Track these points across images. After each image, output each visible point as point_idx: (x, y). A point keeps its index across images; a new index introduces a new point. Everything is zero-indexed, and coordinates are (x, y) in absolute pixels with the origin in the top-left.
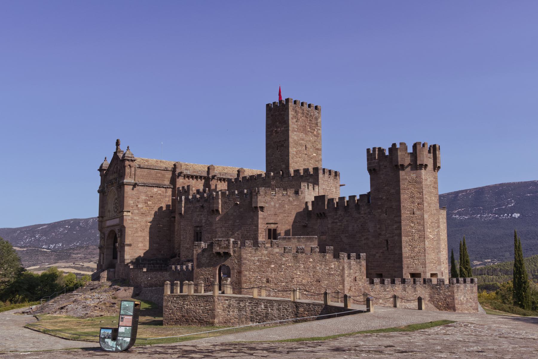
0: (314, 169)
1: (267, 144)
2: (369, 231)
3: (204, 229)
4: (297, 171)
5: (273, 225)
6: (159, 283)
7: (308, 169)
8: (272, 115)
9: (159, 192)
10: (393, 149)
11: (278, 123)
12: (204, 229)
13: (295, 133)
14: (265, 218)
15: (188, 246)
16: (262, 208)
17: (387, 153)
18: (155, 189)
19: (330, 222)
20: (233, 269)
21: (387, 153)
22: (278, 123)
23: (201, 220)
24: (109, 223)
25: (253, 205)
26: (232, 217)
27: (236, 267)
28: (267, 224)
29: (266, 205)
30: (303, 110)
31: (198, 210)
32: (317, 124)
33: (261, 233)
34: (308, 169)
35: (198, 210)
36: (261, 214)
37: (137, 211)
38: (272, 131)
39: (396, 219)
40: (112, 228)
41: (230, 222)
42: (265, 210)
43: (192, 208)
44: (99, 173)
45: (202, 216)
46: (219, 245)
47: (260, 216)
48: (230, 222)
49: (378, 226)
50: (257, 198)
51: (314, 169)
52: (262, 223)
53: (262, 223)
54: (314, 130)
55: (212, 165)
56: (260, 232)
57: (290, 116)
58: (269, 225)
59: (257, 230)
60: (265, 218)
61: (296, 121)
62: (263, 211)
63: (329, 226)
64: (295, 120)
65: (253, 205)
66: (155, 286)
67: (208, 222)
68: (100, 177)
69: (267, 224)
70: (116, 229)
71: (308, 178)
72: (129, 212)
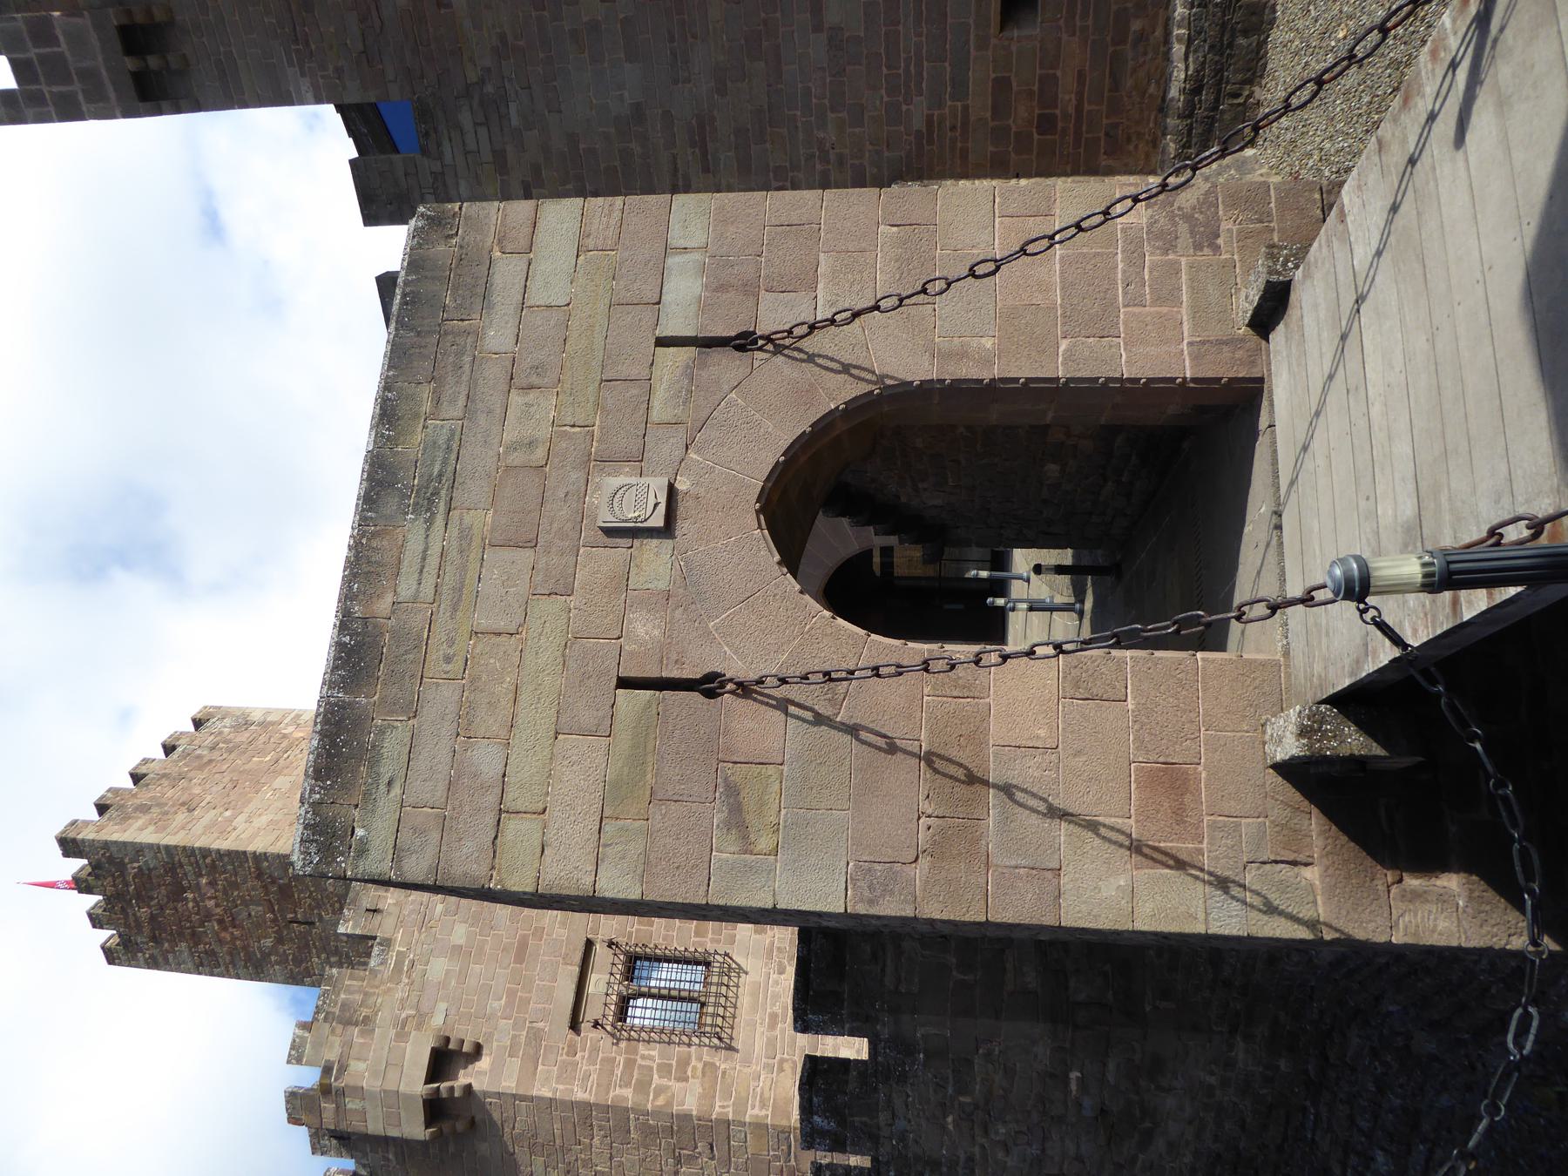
2: (638, 112)
5: (597, 983)
13: (241, 818)
14: (536, 1037)
16: (443, 1060)
25: (415, 1128)
28: (575, 1025)
29: (438, 1020)
30: (164, 776)
32: (264, 725)
33: (643, 1086)
36: (497, 1068)
42: (466, 1034)
47: (509, 1084)
50: (359, 1092)
52: (568, 1072)
53: (568, 1072)
54: (285, 736)
56: (627, 1095)
57: (148, 836)
58: (591, 1011)
59: (616, 1120)
60: (536, 1037)
61: (191, 810)
62: (478, 1051)
64: (181, 817)
65: (415, 1128)
69: (575, 1025)
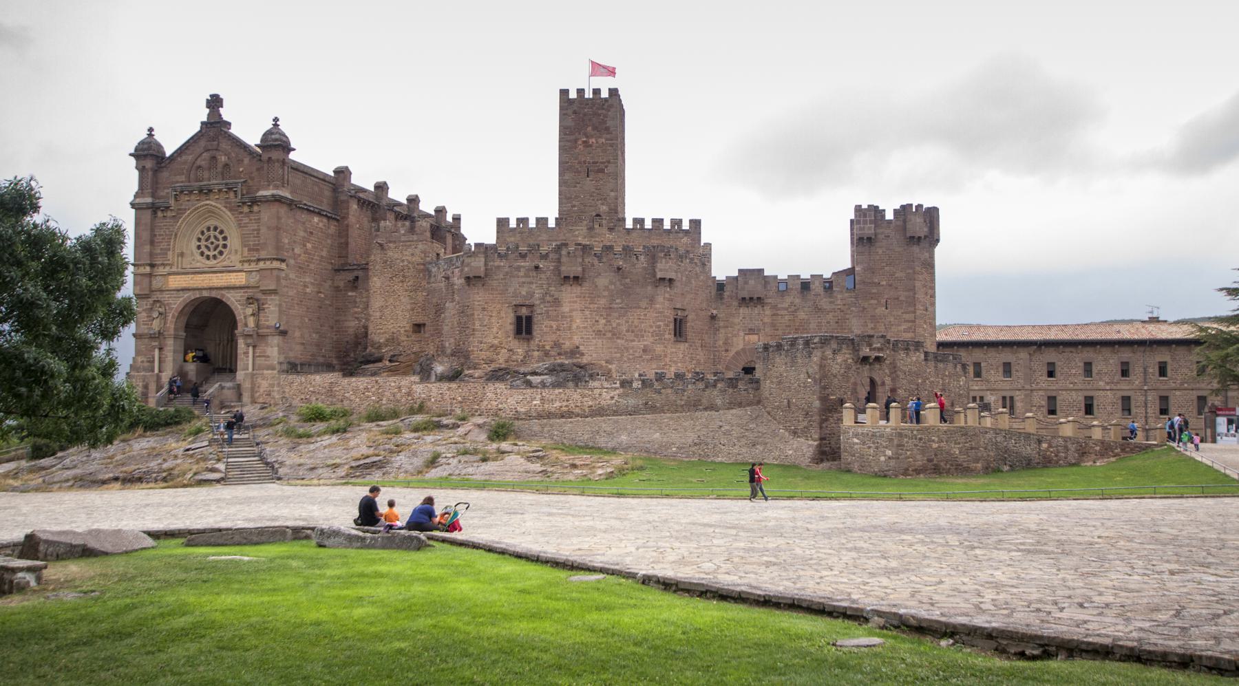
0: (691, 221)
1: (563, 165)
3: (539, 311)
4: (639, 221)
6: (577, 410)
7: (681, 221)
8: (575, 112)
9: (321, 225)
10: (904, 212)
11: (590, 128)
12: (539, 311)
15: (496, 342)
17: (889, 216)
18: (316, 219)
19: (768, 312)
20: (883, 384)
21: (889, 216)
22: (590, 128)
23: (531, 295)
24: (175, 282)
26: (606, 293)
27: (888, 380)
31: (522, 274)
34: (681, 221)
35: (522, 274)
37: (292, 262)
38: (576, 141)
39: (907, 316)
40: (205, 294)
41: (603, 302)
43: (507, 269)
44: (133, 161)
45: (534, 286)
46: (870, 345)
48: (603, 302)
49: (871, 325)
51: (691, 221)
55: (385, 183)
63: (766, 320)
66: (563, 417)
67: (548, 298)
68: (136, 173)
70: (234, 300)
71: (681, 235)
72: (283, 261)
